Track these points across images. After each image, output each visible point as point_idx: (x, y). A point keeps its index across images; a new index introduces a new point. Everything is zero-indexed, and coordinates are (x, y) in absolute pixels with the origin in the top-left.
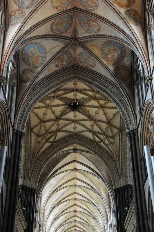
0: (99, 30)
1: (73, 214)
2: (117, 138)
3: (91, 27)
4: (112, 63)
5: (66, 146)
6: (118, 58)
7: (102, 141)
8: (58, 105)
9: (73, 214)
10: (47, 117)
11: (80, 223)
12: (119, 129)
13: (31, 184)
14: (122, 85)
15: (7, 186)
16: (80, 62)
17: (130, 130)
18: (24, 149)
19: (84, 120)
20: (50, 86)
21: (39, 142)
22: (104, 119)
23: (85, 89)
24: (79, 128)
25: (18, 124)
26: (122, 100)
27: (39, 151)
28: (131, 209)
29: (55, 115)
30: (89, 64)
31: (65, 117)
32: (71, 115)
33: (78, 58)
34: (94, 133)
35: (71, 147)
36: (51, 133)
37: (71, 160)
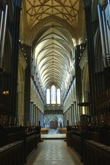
1: (52, 63)
2: (77, 17)
5: (47, 23)
9: (52, 63)
10: (36, 4)
12: (78, 12)
15: (13, 39)
17: (86, 5)
19: (58, 6)
22: (70, 5)
24: (55, 11)
25: (17, 2)
27: (32, 25)
28: (84, 54)
29: (40, 2)
31: (46, 4)
34: (63, 14)
35: (50, 24)
37: (51, 32)
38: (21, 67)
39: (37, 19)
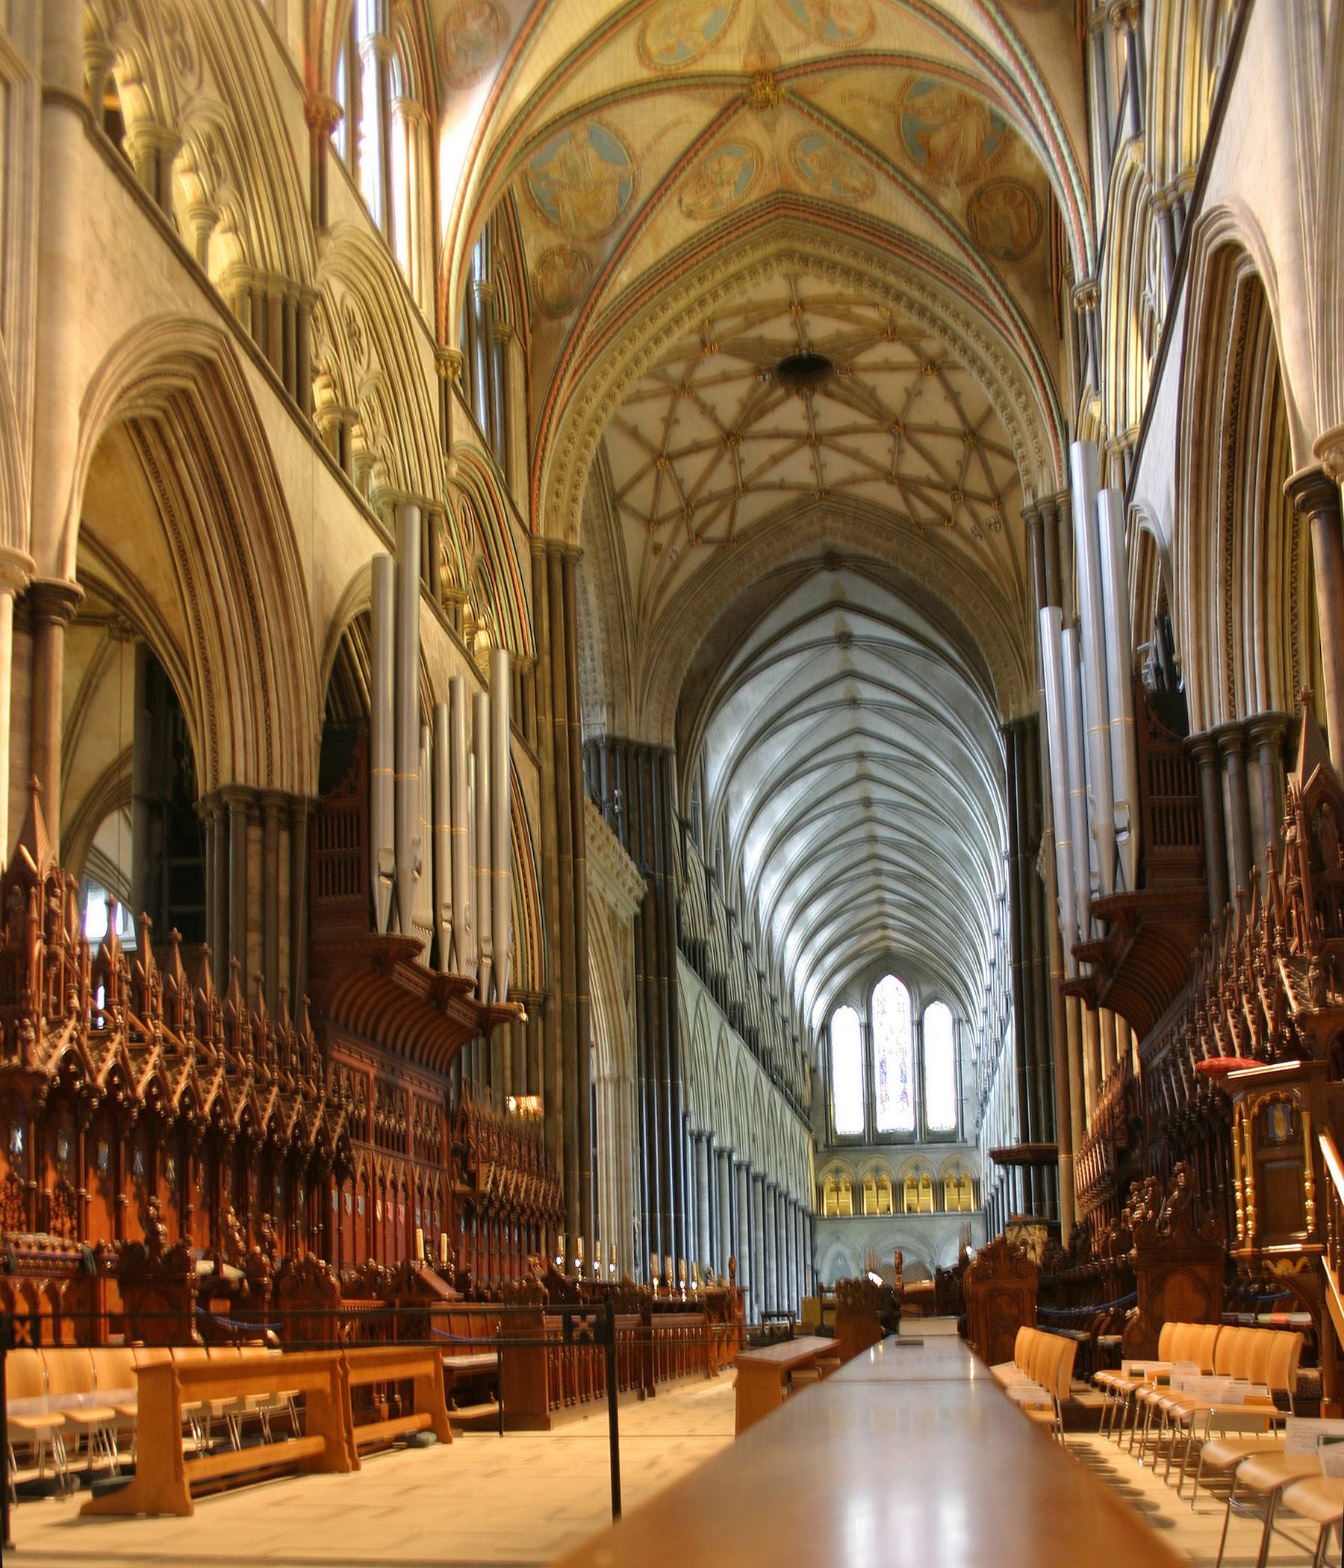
0: (872, 26)
3: (833, 13)
4: (952, 178)
6: (982, 144)
7: (946, 518)
8: (725, 378)
10: (682, 438)
11: (897, 846)
13: (643, 730)
14: (1003, 284)
16: (803, 178)
17: (1040, 495)
18: (596, 586)
19: (854, 430)
20: (670, 311)
21: (657, 549)
22: (949, 418)
23: (839, 299)
24: (838, 468)
26: (1006, 356)
27: (662, 588)
29: (716, 421)
30: (846, 187)
31: (767, 423)
32: (790, 414)
33: (790, 157)
36: (708, 501)
38: (604, 916)
39: (697, 536)
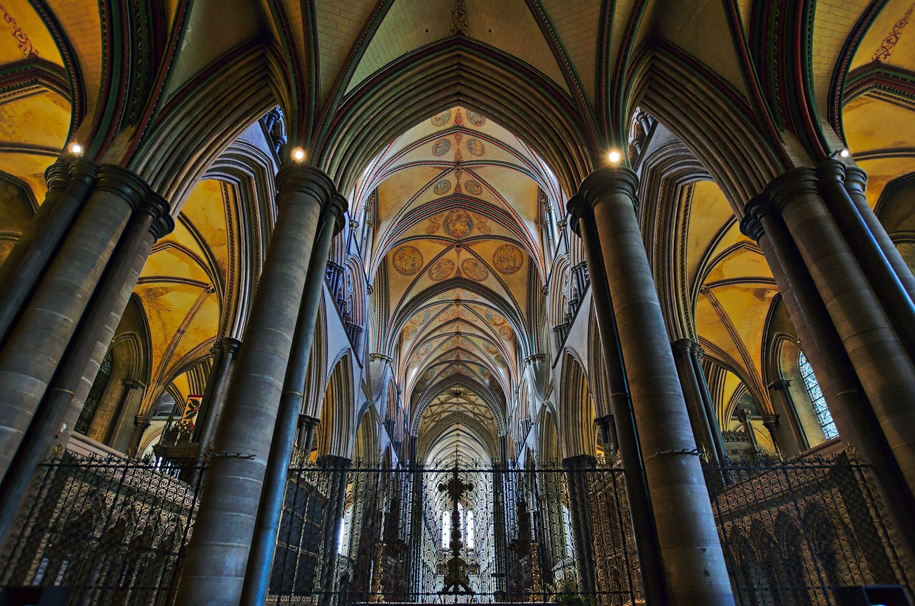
4: (488, 377)
24: (461, 409)
